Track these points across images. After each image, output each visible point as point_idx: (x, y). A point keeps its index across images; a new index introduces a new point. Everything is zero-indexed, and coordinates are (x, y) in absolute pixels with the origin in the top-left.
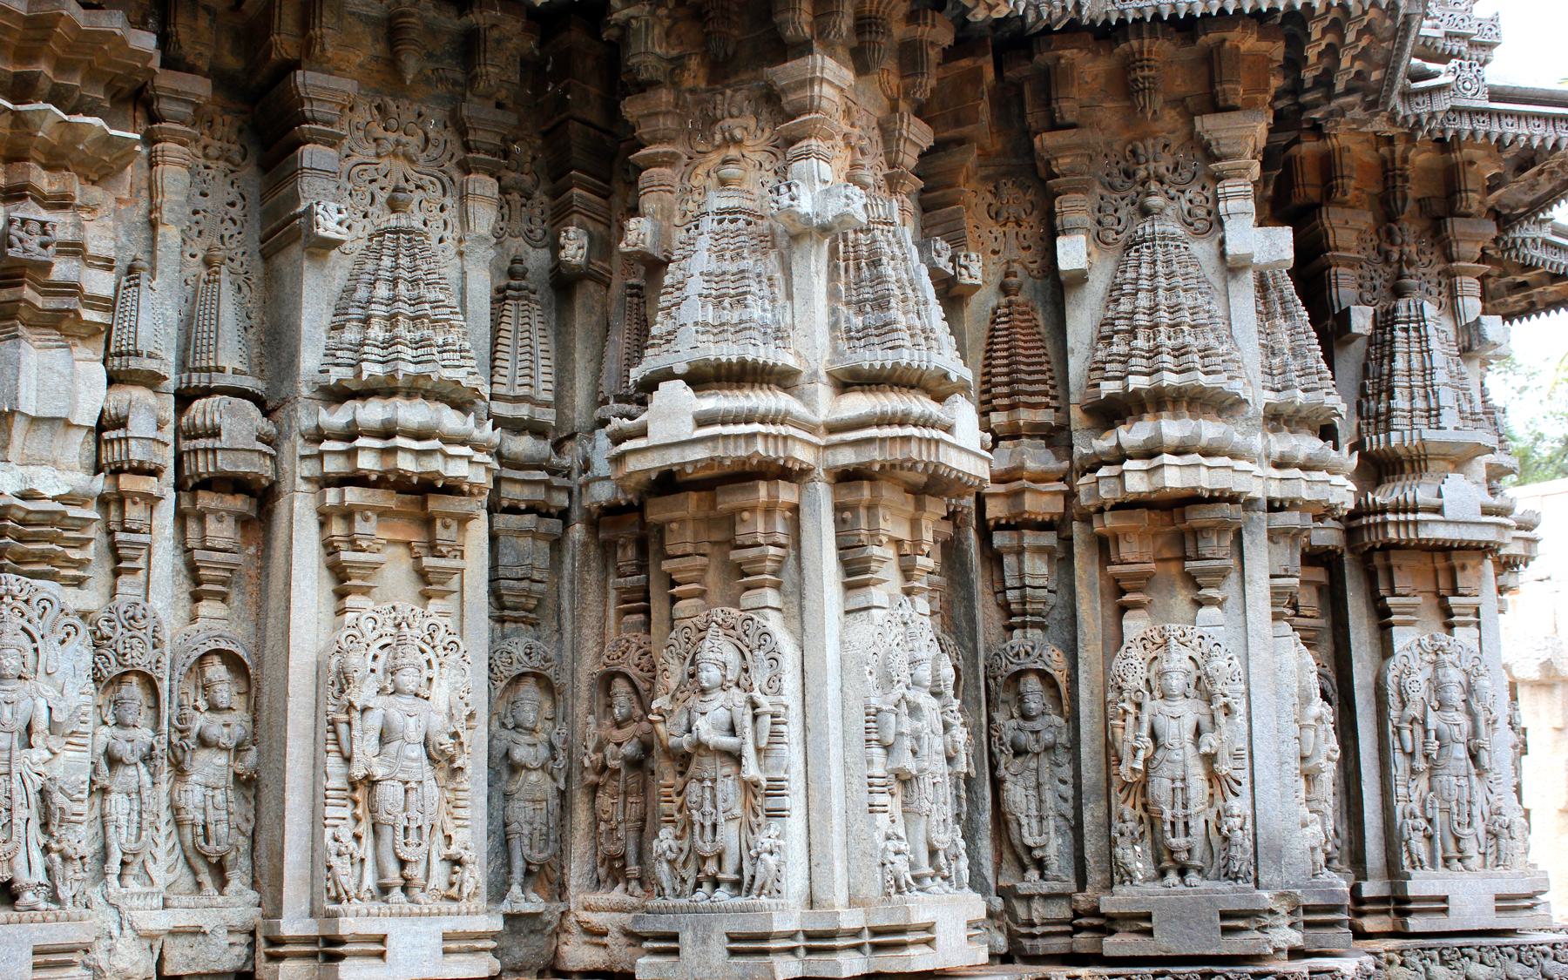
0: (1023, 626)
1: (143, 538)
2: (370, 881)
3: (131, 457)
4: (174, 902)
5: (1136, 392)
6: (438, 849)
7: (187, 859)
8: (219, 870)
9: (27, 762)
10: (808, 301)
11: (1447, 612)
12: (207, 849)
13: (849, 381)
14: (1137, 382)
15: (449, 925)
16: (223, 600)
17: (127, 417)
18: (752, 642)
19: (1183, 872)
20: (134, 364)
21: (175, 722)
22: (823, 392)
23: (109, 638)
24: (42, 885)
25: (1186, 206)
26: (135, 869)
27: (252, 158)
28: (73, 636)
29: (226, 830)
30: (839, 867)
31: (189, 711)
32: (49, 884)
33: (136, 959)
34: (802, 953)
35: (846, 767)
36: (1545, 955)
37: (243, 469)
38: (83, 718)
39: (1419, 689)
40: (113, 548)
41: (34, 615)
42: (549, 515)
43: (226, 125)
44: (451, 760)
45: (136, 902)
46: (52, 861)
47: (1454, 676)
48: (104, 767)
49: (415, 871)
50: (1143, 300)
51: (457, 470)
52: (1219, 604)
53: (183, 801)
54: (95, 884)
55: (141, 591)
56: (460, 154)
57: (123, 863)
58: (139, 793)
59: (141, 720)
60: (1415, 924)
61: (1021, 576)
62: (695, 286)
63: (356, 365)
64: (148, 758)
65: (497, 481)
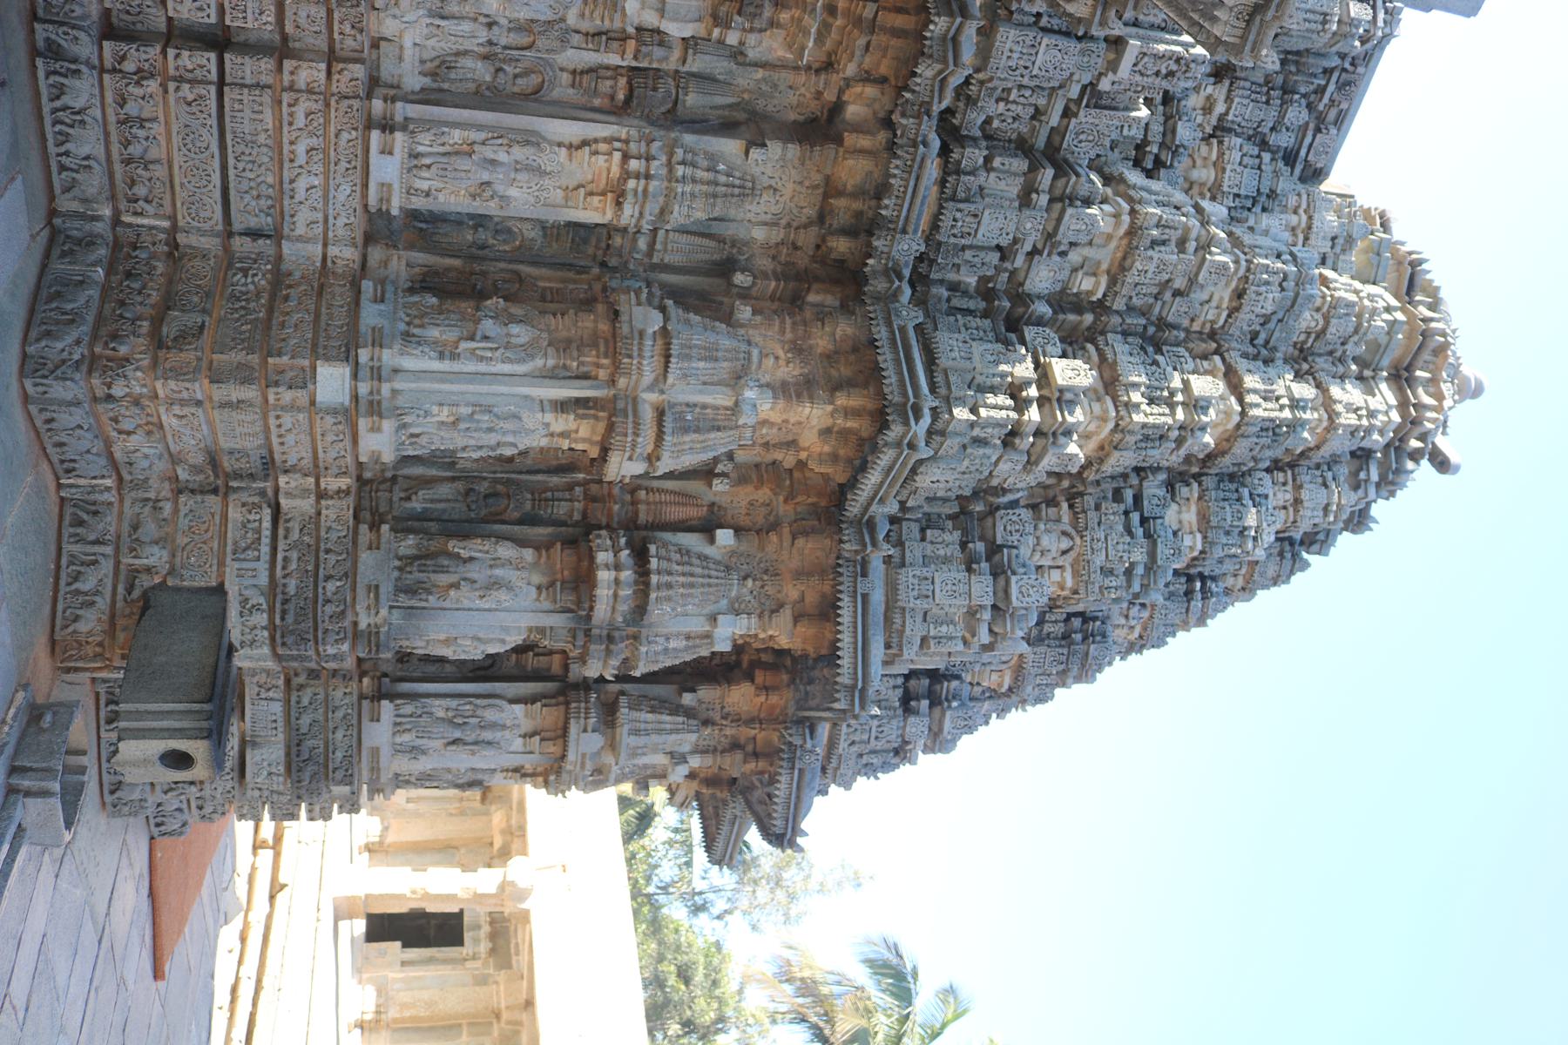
0: (534, 500)
1: (602, 49)
2: (421, 149)
4: (417, 49)
5: (649, 562)
6: (436, 184)
8: (434, 74)
10: (701, 392)
11: (532, 735)
13: (660, 413)
14: (654, 563)
15: (396, 186)
18: (528, 351)
19: (400, 569)
20: (690, 51)
22: (653, 397)
25: (747, 599)
26: (435, 31)
27: (801, 118)
30: (413, 385)
34: (371, 364)
35: (462, 393)
36: (347, 770)
39: (490, 715)
40: (599, 34)
42: (605, 255)
43: (814, 107)
44: (480, 195)
47: (497, 735)
48: (488, 20)
49: (425, 174)
50: (699, 571)
51: (628, 210)
52: (538, 599)
55: (576, 45)
56: (795, 224)
59: (510, 40)
60: (365, 703)
61: (560, 500)
62: (712, 338)
63: (683, 163)
64: (490, 43)
65: (625, 230)
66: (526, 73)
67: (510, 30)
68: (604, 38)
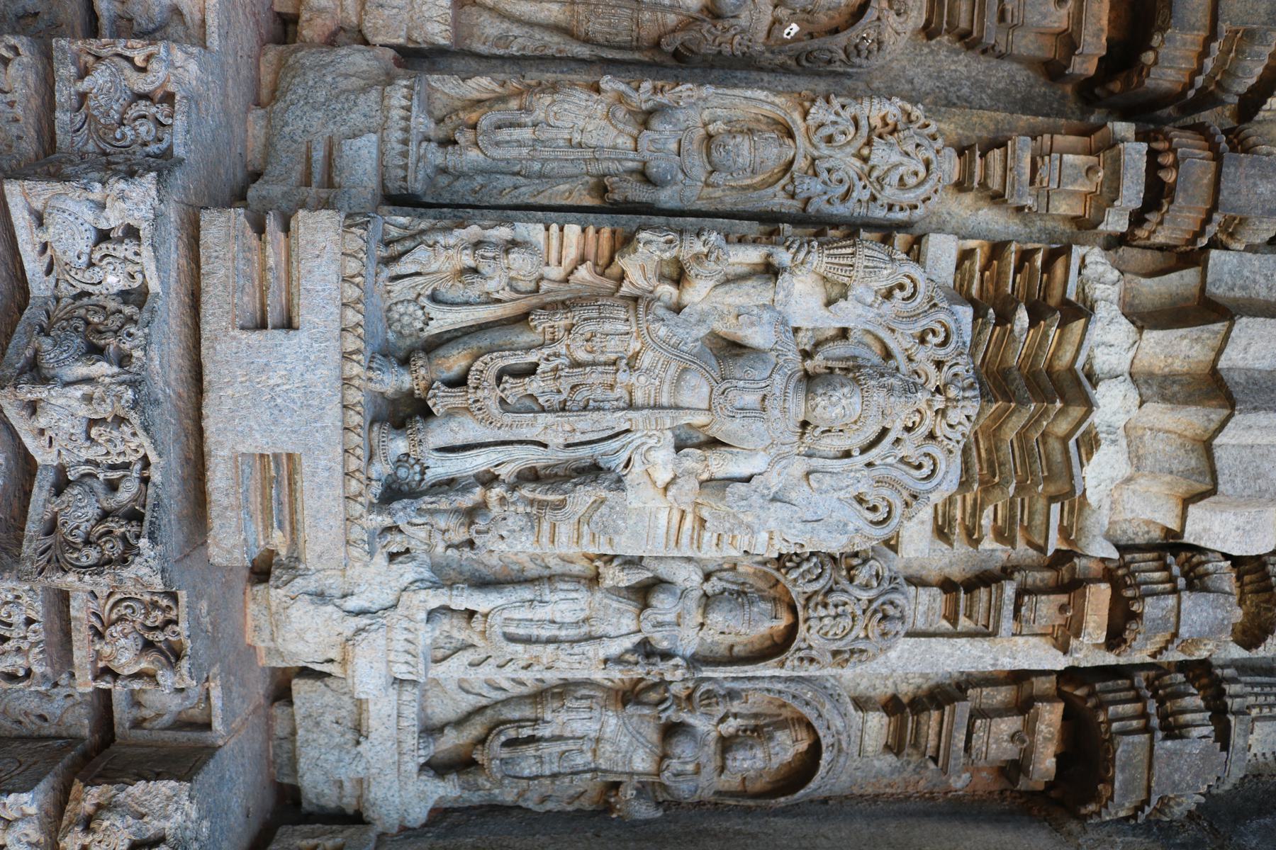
3: (1149, 600)
7: (480, 710)
9: (652, 442)
12: (496, 743)
16: (888, 748)
17: (1206, 589)
21: (705, 687)
23: (851, 580)
24: (423, 473)
28: (870, 516)
29: (526, 773)
31: (720, 710)
32: (424, 486)
33: (309, 636)
37: (1119, 778)
38: (726, 538)
41: (906, 450)
45: (399, 635)
46: (466, 489)
53: (576, 704)
54: (435, 568)
55: (921, 625)
57: (471, 614)
58: (589, 638)
66: (758, 731)
67: (708, 602)
68: (1009, 589)
